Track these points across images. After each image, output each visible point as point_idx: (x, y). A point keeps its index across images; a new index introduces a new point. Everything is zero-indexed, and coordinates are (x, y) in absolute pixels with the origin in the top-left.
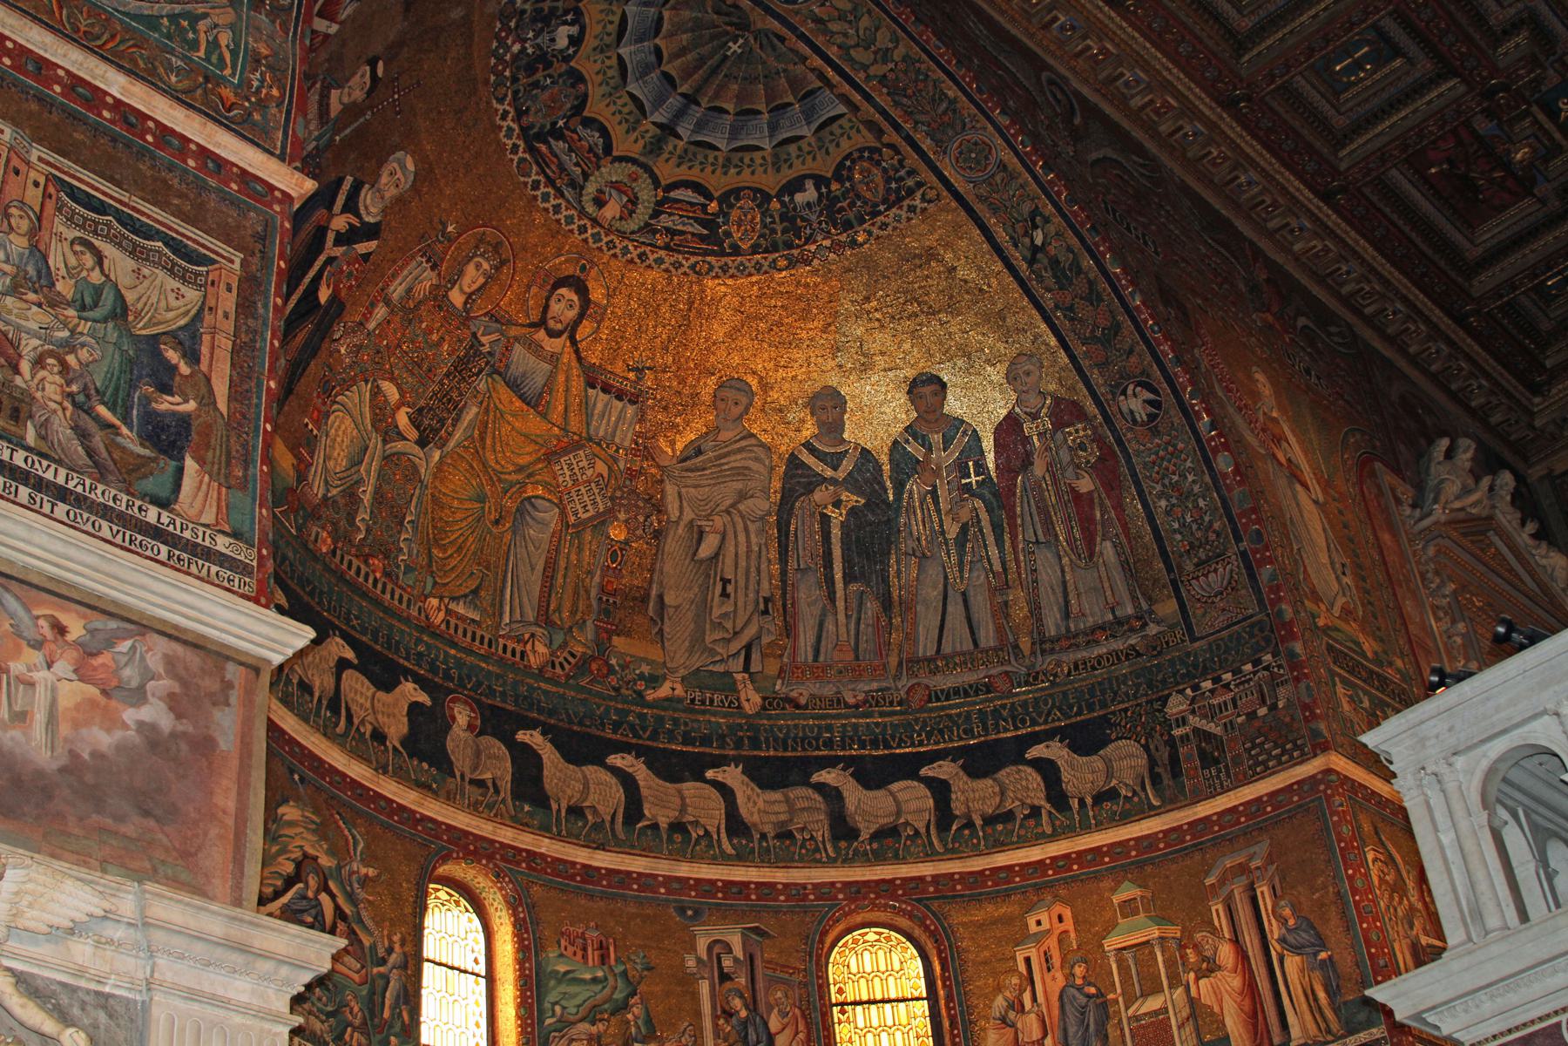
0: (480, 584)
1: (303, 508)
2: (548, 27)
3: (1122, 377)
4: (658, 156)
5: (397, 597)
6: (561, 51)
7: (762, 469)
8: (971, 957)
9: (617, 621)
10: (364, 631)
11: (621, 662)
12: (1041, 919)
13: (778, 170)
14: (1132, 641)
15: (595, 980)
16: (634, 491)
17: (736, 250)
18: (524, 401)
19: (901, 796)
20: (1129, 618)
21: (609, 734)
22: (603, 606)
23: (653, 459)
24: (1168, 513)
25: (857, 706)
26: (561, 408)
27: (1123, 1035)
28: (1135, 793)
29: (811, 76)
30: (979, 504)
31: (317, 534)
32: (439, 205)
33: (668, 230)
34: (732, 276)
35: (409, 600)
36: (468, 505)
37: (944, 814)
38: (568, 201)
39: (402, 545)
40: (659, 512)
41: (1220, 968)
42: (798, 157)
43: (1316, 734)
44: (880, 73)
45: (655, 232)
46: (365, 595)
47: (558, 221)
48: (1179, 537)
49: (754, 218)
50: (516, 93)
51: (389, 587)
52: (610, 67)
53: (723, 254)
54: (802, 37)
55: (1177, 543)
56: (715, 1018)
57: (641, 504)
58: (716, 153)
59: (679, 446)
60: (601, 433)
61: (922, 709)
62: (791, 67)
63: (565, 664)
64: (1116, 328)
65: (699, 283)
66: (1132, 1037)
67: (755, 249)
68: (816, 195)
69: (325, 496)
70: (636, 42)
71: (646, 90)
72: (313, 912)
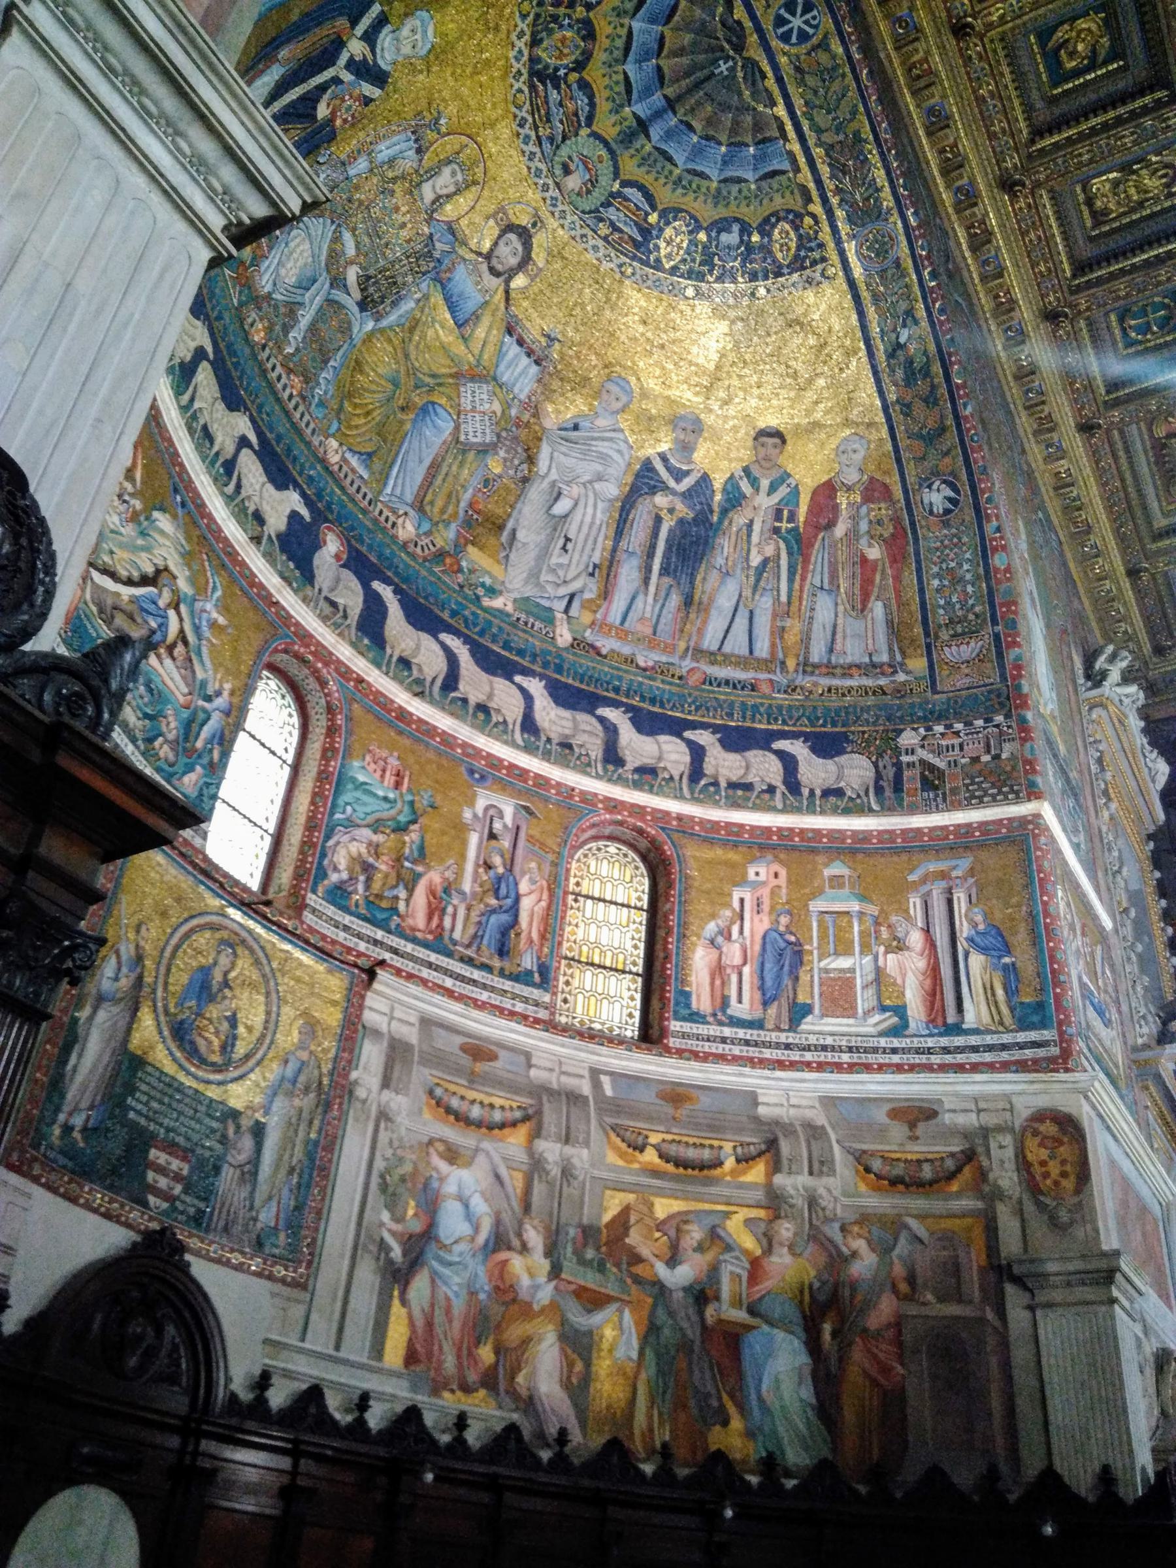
3: (932, 473)
7: (620, 461)
8: (696, 884)
10: (271, 430)
12: (760, 871)
14: (882, 681)
15: (385, 799)
17: (658, 266)
19: (665, 747)
20: (882, 665)
21: (446, 615)
24: (938, 591)
25: (645, 670)
27: (812, 981)
28: (859, 796)
30: (782, 545)
37: (696, 772)
41: (908, 948)
43: (1032, 784)
44: (829, 141)
45: (601, 220)
46: (278, 400)
48: (941, 612)
50: (538, 16)
51: (301, 408)
53: (646, 263)
55: (942, 616)
56: (477, 865)
61: (696, 688)
62: (761, 108)
64: (943, 430)
65: (621, 282)
66: (821, 985)
72: (160, 620)
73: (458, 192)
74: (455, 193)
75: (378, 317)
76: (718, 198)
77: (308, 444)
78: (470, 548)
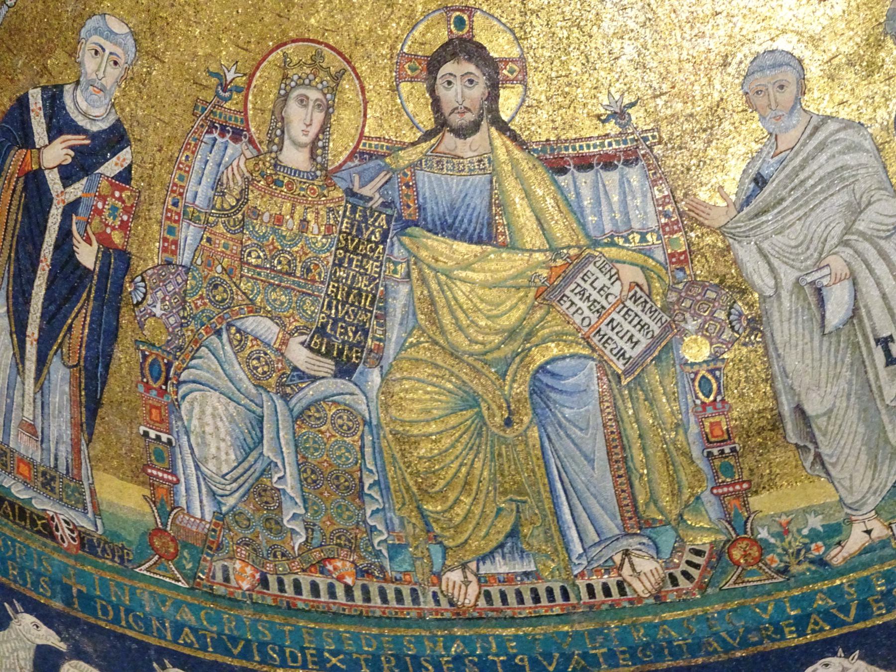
0: (518, 518)
1: (185, 546)
5: (391, 595)
7: (864, 158)
9: (746, 475)
11: (776, 529)
16: (693, 283)
18: (471, 241)
21: (793, 640)
22: (717, 463)
23: (702, 225)
26: (532, 224)
31: (225, 569)
32: (195, 55)
35: (414, 591)
36: (453, 421)
39: (371, 522)
40: (743, 292)
46: (336, 617)
57: (711, 295)
59: (731, 189)
60: (608, 227)
63: (692, 570)
69: (219, 516)
73: (328, 110)
74: (328, 116)
75: (377, 357)
78: (755, 502)
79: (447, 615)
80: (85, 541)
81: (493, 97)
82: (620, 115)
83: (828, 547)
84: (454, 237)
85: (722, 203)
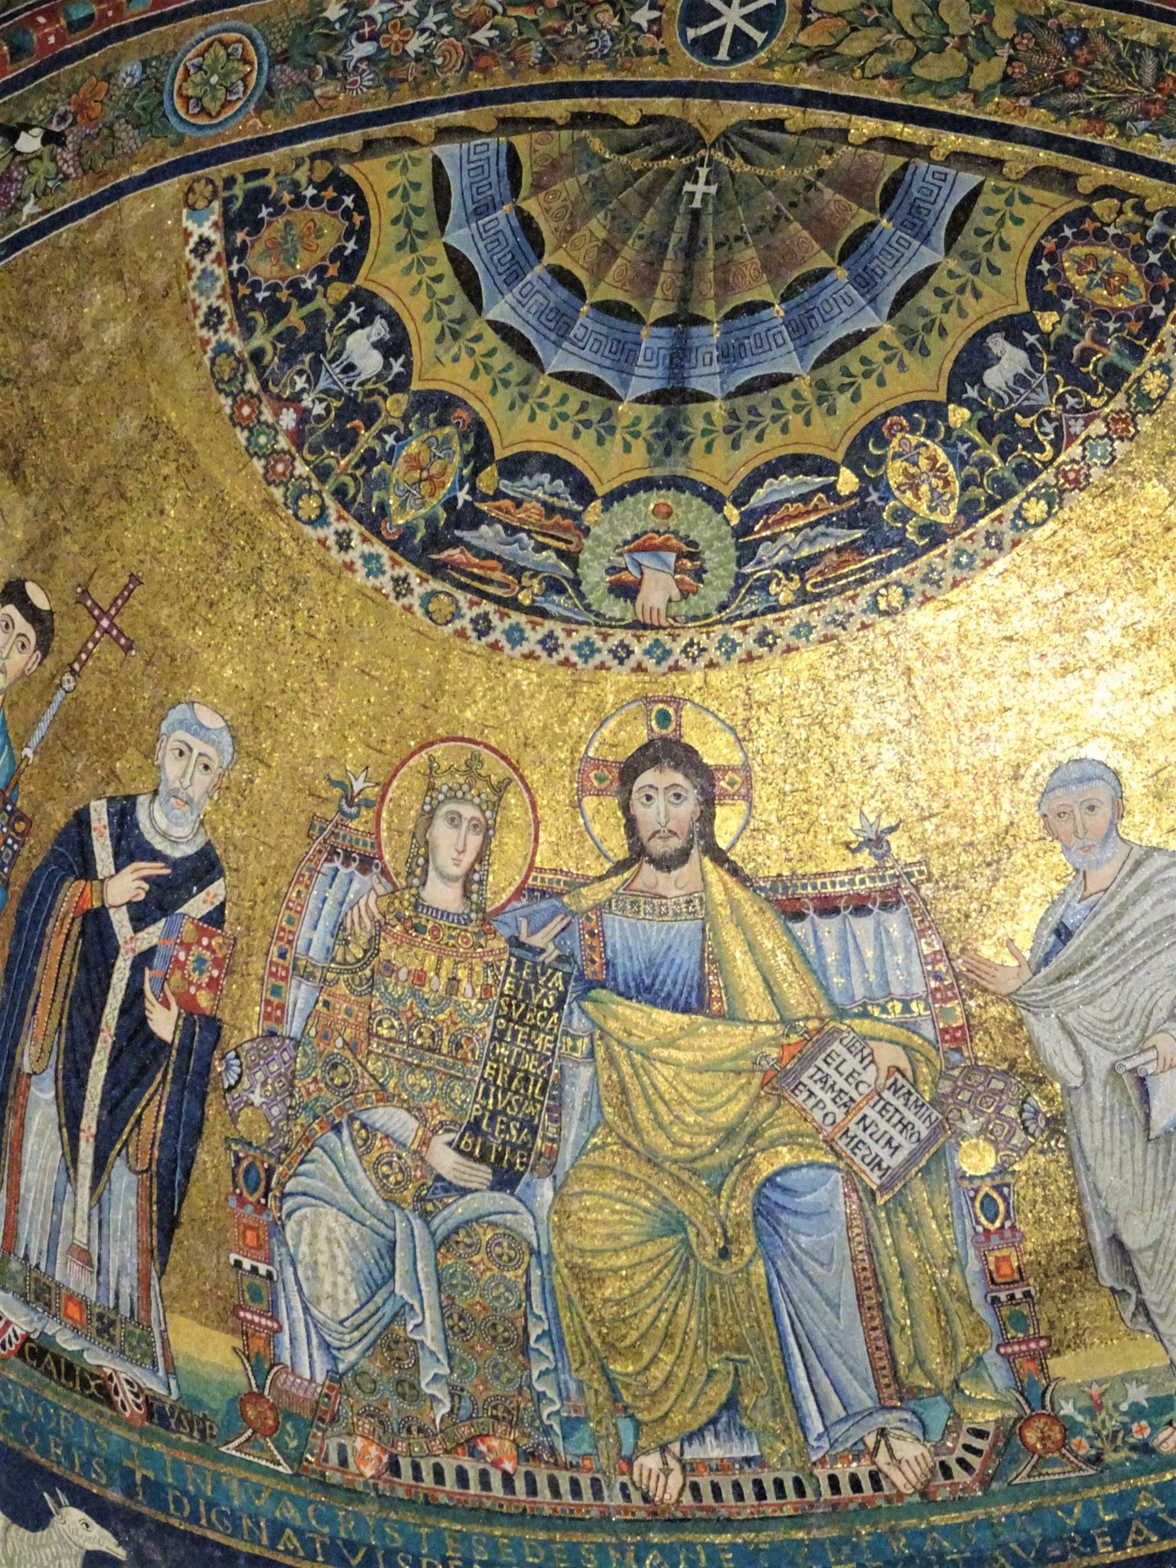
0: (737, 1384)
1: (289, 1416)
2: (324, 351)
4: (686, 449)
5: (565, 1487)
6: (379, 377)
9: (1044, 1329)
11: (1084, 1402)
13: (925, 352)
18: (675, 1009)
22: (1005, 1311)
23: (985, 990)
29: (875, 156)
31: (342, 1449)
32: (312, 757)
33: (786, 567)
34: (955, 584)
35: (595, 1482)
36: (650, 1250)
38: (567, 620)
39: (539, 1387)
40: (1040, 1081)
42: (946, 308)
45: (764, 584)
46: (491, 1516)
47: (566, 662)
49: (933, 459)
50: (340, 493)
52: (491, 353)
53: (914, 553)
54: (808, 100)
57: (998, 1085)
58: (791, 386)
59: (1024, 943)
60: (860, 993)
62: (826, 162)
63: (970, 1458)
67: (969, 513)
68: (1022, 356)
69: (335, 1377)
70: (509, 284)
71: (585, 353)
73: (487, 832)
74: (486, 841)
76: (915, 343)
77: (603, 1522)
78: (1056, 1366)
79: (641, 1515)
80: (154, 1410)
81: (707, 817)
82: (876, 843)
83: (1155, 1429)
84: (654, 1004)
85: (1012, 963)
